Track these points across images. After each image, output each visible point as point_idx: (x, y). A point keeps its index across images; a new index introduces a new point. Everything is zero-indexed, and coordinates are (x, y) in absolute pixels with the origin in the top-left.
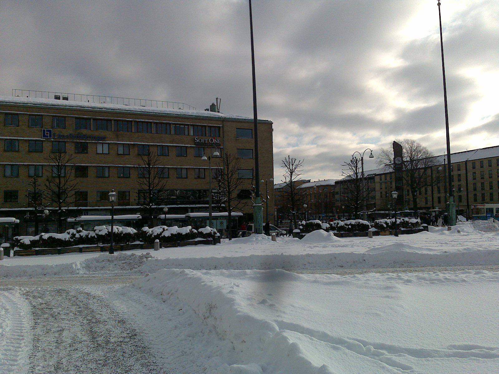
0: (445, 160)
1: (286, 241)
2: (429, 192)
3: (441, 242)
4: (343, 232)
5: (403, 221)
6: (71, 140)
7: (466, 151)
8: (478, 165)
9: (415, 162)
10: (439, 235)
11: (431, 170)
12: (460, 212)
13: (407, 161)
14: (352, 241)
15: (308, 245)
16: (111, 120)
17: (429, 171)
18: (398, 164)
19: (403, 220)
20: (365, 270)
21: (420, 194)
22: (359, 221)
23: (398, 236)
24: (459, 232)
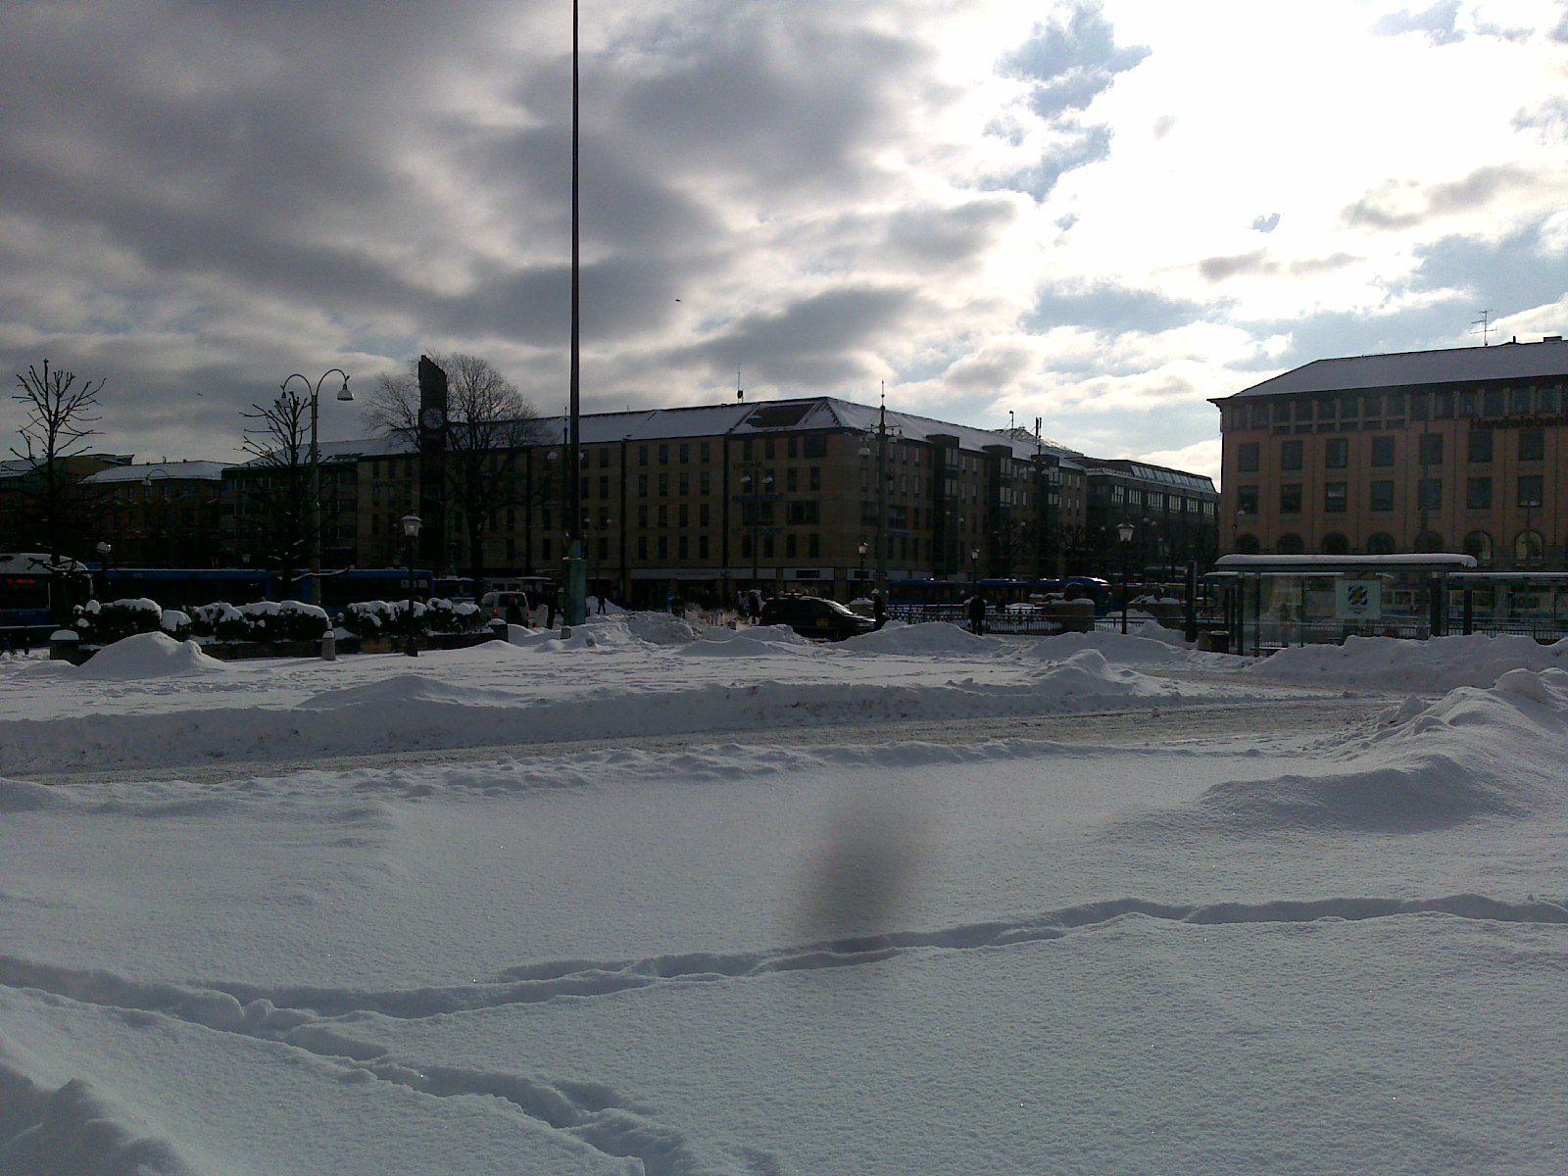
0: (566, 430)
1: (22, 673)
2: (520, 526)
3: (537, 672)
4: (234, 642)
5: (434, 609)
7: (626, 411)
8: (653, 455)
9: (482, 428)
10: (537, 651)
11: (529, 457)
12: (602, 590)
13: (458, 424)
14: (267, 672)
15: (103, 686)
17: (521, 462)
18: (433, 431)
19: (435, 604)
20: (295, 764)
21: (493, 524)
22: (292, 607)
23: (417, 656)
24: (591, 643)
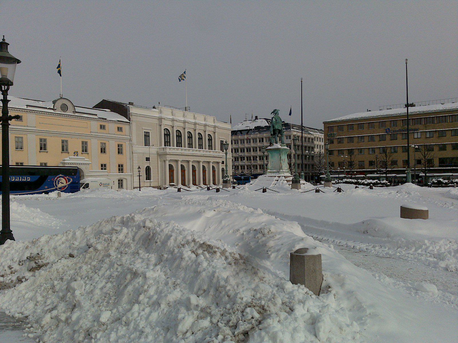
6: (400, 133)
16: (422, 118)
